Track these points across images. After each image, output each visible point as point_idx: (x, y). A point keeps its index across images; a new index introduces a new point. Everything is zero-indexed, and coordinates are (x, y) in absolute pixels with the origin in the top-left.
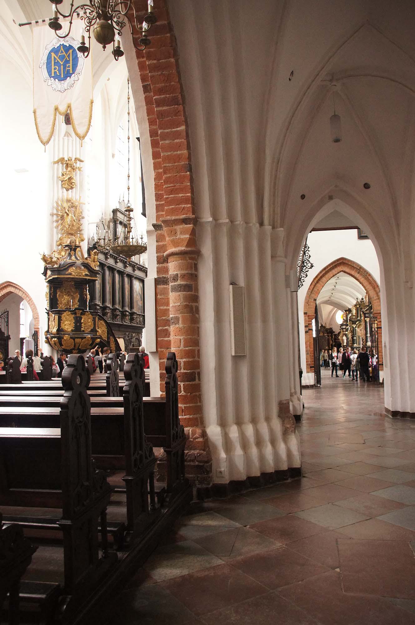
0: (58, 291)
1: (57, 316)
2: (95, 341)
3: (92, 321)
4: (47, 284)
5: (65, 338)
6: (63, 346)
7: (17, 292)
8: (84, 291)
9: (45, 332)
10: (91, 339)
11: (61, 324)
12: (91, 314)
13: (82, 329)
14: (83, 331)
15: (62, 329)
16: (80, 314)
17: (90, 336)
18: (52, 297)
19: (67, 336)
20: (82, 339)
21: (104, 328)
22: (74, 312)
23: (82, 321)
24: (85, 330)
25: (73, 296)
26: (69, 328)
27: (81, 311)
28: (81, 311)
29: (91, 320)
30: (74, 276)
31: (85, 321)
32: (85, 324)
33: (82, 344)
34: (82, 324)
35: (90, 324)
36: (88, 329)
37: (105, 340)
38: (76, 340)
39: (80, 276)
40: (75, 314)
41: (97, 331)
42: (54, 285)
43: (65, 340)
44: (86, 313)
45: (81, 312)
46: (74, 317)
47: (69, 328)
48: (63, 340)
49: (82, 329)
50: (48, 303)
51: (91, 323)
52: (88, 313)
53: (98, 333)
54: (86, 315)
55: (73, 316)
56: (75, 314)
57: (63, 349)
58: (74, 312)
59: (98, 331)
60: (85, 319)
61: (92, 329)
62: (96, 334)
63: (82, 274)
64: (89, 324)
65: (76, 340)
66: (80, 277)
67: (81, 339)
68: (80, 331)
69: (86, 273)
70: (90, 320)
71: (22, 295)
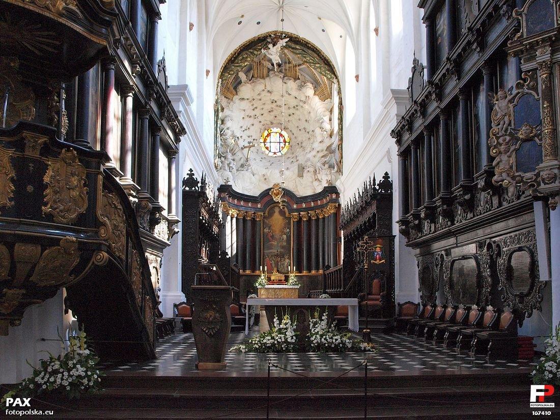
2: (93, 259)
3: (85, 185)
8: (53, 99)
10: (80, 249)
12: (80, 161)
13: (46, 209)
14: (50, 217)
16: (39, 148)
17: (74, 239)
20: (42, 246)
21: (118, 218)
22: (15, 138)
23: (46, 179)
24: (55, 213)
27: (42, 140)
28: (42, 140)
29: (79, 181)
31: (58, 181)
32: (56, 192)
33: (42, 264)
34: (48, 191)
35: (75, 193)
36: (68, 210)
37: (119, 257)
38: (19, 248)
39: (47, 8)
40: (20, 145)
41: (98, 224)
44: (64, 150)
45: (45, 143)
46: (12, 160)
49: (46, 209)
51: (81, 192)
52: (69, 154)
53: (102, 231)
54: (63, 160)
55: (11, 152)
56: (20, 145)
58: (15, 138)
59: (104, 224)
60: (57, 172)
61: (82, 214)
62: (97, 233)
63: (54, 6)
64: (75, 193)
65: (19, 248)
66: (47, 14)
67: (39, 248)
68: (36, 214)
69: (70, 6)
70: (75, 181)
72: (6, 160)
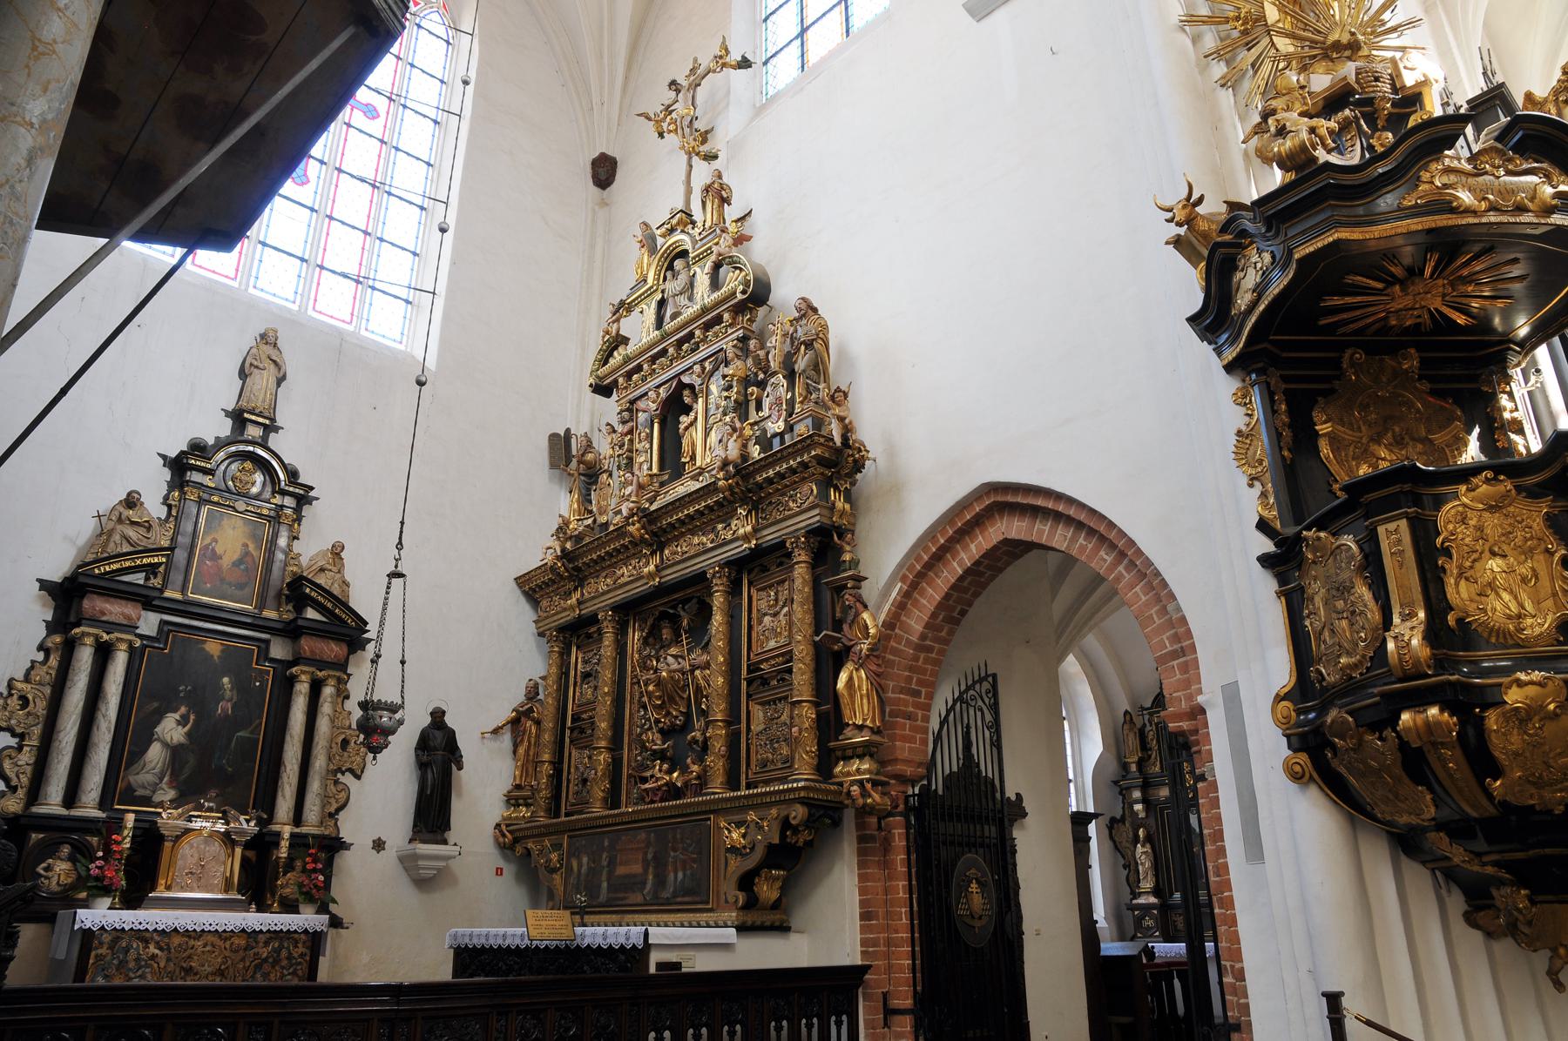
0: (1317, 416)
1: (1403, 523)
4: (1229, 385)
5: (1513, 697)
6: (1497, 772)
7: (1041, 532)
9: (1279, 699)
11: (1450, 581)
15: (1460, 621)
18: (1286, 453)
19: (1537, 675)
25: (1431, 441)
26: (1529, 606)
30: (1474, 213)
42: (1285, 379)
43: (1522, 717)
47: (1529, 606)
48: (1492, 720)
50: (1264, 495)
57: (1504, 805)
71: (1073, 540)
72: (1538, 523)
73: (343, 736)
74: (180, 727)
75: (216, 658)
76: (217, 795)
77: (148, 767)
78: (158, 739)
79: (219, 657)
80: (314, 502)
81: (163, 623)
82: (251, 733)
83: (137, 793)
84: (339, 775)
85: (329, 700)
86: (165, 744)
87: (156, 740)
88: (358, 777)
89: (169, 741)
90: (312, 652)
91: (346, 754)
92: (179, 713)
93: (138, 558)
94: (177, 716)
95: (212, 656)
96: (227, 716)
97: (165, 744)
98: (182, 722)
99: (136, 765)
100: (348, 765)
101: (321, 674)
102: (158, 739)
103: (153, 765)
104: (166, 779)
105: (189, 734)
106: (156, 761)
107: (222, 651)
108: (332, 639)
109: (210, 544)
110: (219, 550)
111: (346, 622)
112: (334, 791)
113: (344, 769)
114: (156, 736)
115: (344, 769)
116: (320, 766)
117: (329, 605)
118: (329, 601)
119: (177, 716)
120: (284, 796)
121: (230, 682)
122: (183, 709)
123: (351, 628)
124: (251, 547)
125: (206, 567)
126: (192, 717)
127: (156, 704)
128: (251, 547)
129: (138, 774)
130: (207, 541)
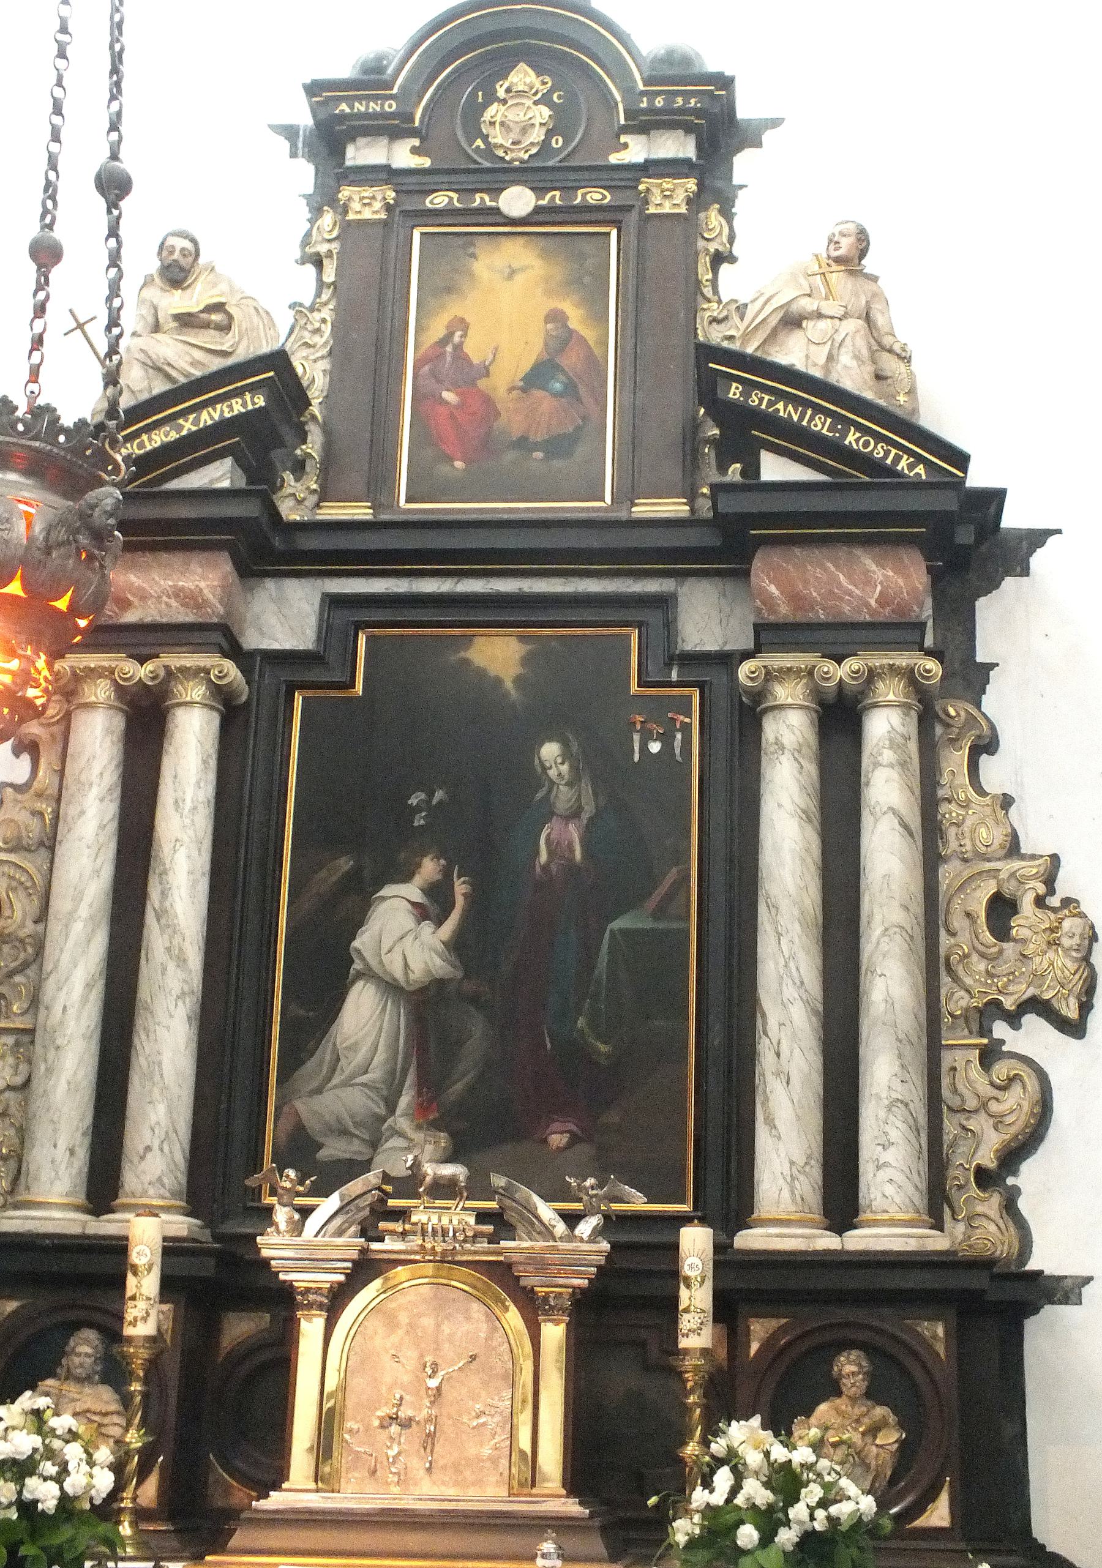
73: (989, 888)
74: (427, 927)
75: (509, 685)
76: (574, 1140)
77: (350, 1064)
78: (367, 974)
79: (518, 680)
80: (767, 137)
81: (333, 602)
82: (659, 913)
83: (323, 1154)
84: (1000, 1030)
85: (888, 756)
86: (390, 987)
87: (359, 975)
88: (1075, 1028)
89: (399, 974)
90: (797, 600)
91: (1009, 947)
92: (418, 880)
93: (183, 414)
94: (412, 891)
95: (498, 681)
96: (571, 868)
97: (390, 987)
98: (433, 910)
99: (310, 1065)
100: (1022, 990)
101: (844, 671)
102: (367, 974)
103: (360, 1056)
104: (405, 1101)
105: (457, 946)
106: (370, 1040)
107: (526, 661)
108: (867, 541)
109: (448, 337)
110: (475, 348)
111: (891, 472)
112: (988, 1091)
113: (1009, 1003)
114: (357, 965)
115: (1009, 1003)
116: (889, 1002)
117: (821, 425)
118: (818, 409)
119: (412, 891)
120: (771, 1123)
121: (566, 755)
122: (429, 868)
123: (917, 485)
124: (576, 317)
125: (442, 411)
126: (461, 888)
127: (345, 864)
128: (576, 317)
129: (319, 1091)
130: (437, 330)
